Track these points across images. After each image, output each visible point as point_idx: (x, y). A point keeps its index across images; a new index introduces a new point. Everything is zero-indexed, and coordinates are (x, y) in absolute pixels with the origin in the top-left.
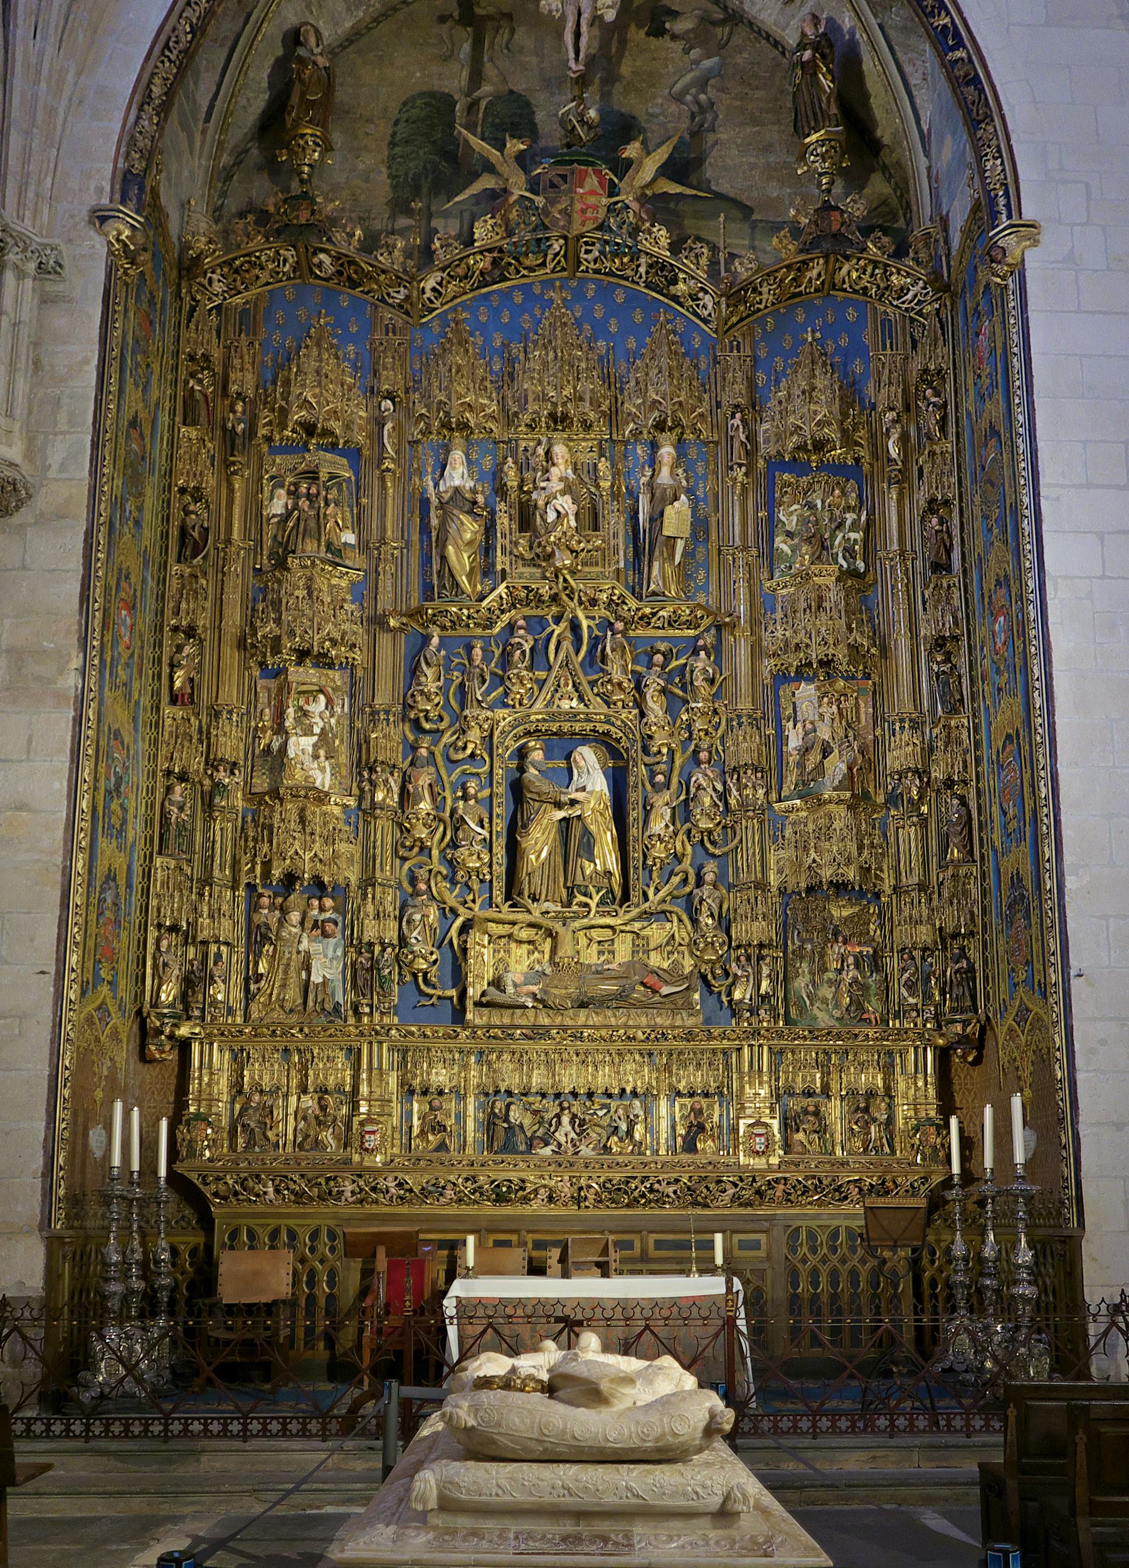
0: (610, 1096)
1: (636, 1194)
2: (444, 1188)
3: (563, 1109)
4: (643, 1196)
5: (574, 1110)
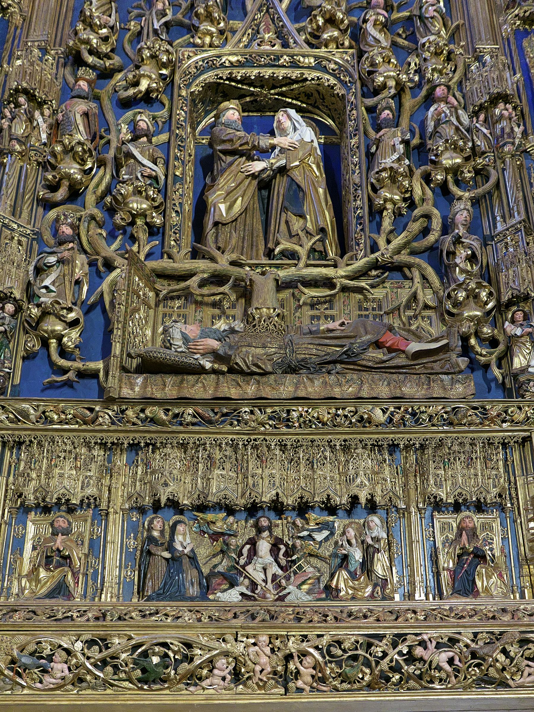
0: (332, 510)
1: (384, 664)
2: (50, 658)
3: (259, 530)
4: (396, 669)
5: (278, 532)
